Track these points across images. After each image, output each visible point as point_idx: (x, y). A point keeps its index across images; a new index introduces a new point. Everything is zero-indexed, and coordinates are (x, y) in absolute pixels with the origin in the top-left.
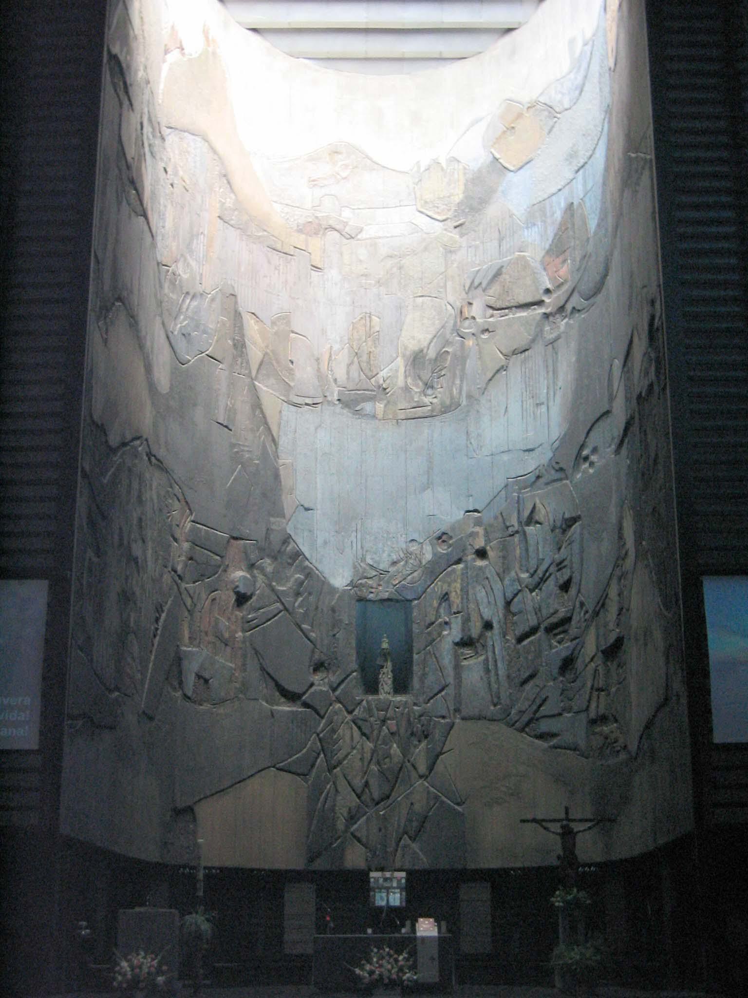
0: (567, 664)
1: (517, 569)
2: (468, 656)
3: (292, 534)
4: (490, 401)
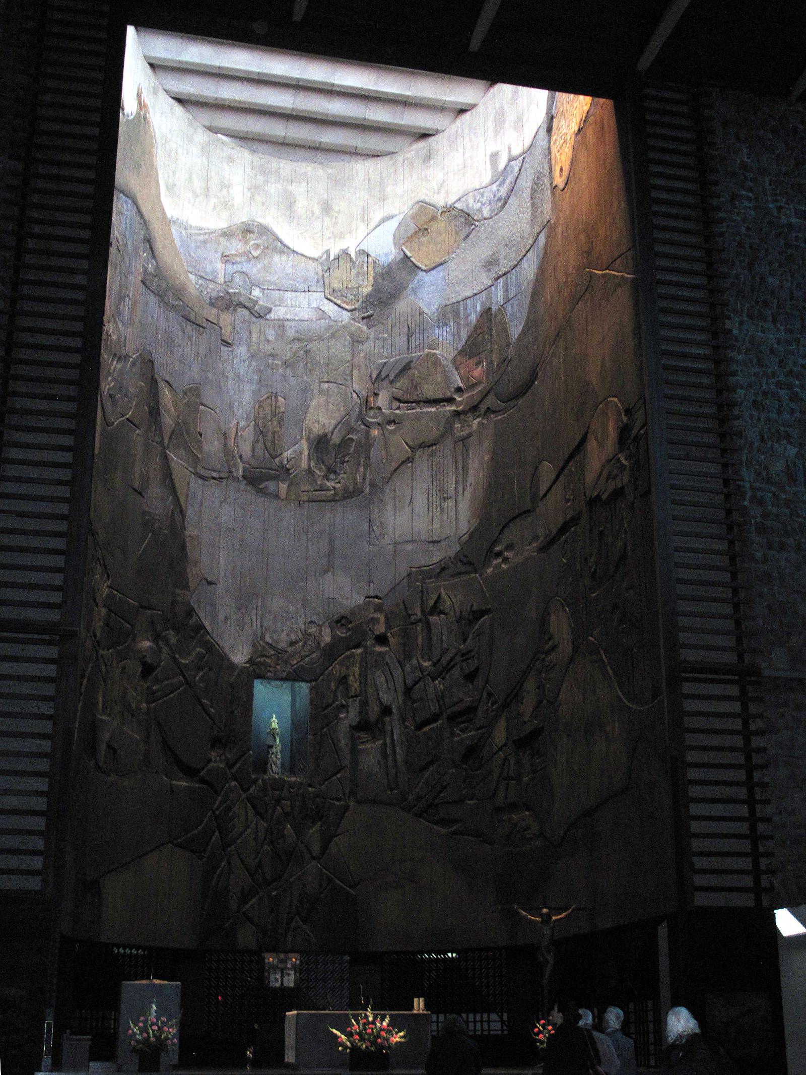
0: (472, 752)
1: (419, 656)
2: (365, 740)
3: (195, 606)
4: (394, 490)
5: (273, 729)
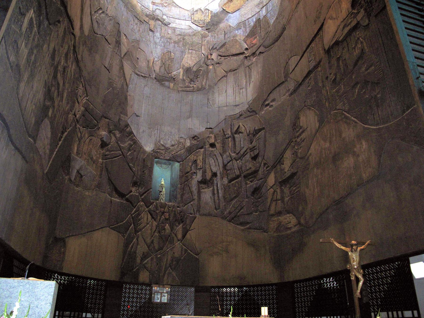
0: (256, 191)
1: (230, 151)
3: (130, 124)
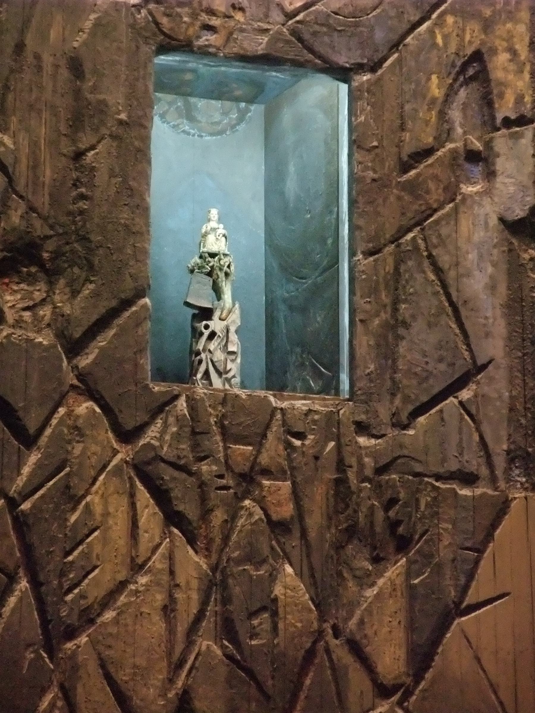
5: (213, 255)
